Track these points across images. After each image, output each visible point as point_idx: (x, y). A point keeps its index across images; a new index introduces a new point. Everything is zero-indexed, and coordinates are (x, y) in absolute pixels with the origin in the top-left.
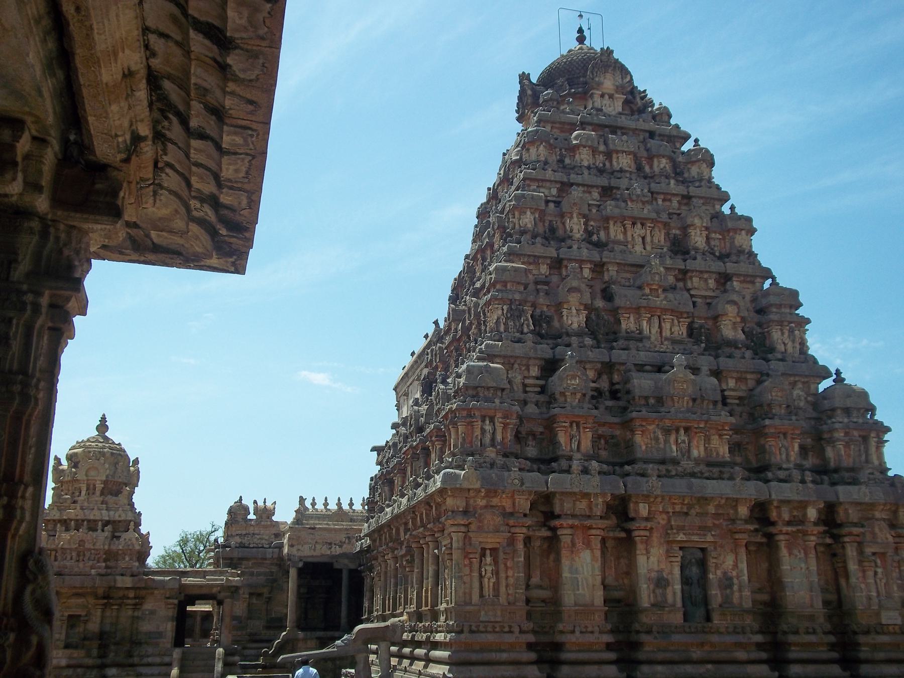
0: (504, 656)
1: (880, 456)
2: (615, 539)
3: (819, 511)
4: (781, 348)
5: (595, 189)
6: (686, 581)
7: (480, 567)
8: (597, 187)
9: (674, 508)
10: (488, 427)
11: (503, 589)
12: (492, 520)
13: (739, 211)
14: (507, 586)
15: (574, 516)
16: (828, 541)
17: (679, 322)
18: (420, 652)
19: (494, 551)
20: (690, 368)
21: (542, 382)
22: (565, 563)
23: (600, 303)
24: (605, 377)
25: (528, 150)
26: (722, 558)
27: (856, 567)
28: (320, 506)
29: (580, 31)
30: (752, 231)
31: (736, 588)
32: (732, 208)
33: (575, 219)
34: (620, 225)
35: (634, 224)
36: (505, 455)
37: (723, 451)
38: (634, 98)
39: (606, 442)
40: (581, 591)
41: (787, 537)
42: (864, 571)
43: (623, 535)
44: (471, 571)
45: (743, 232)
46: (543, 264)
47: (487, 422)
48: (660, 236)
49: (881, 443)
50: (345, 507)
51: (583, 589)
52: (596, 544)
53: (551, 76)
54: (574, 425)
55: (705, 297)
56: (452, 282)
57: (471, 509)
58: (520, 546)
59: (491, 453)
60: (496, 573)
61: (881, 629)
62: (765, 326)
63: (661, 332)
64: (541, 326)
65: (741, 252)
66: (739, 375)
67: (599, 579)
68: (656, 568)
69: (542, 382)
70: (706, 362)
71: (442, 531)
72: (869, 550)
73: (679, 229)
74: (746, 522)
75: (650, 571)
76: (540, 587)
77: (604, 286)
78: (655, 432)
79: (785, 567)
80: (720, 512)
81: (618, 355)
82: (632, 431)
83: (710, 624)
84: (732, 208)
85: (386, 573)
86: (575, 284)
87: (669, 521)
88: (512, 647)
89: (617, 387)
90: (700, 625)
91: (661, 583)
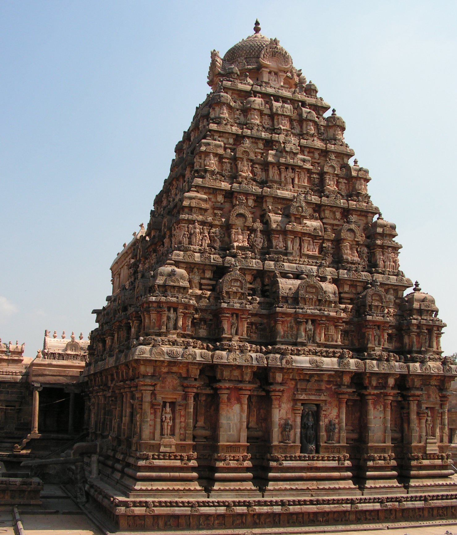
1: (438, 343)
2: (258, 396)
3: (396, 380)
5: (260, 141)
6: (304, 426)
7: (162, 415)
8: (262, 139)
10: (172, 315)
12: (172, 382)
13: (360, 165)
14: (180, 428)
15: (230, 380)
16: (400, 399)
17: (313, 242)
18: (118, 466)
19: (173, 405)
20: (319, 277)
21: (214, 282)
23: (258, 225)
24: (259, 280)
25: (214, 109)
26: (329, 411)
27: (415, 417)
29: (257, 23)
30: (367, 180)
31: (337, 430)
32: (356, 162)
34: (276, 168)
35: (287, 168)
36: (184, 336)
38: (292, 75)
39: (256, 328)
41: (374, 397)
42: (420, 419)
43: (263, 393)
44: (155, 417)
46: (220, 194)
47: (172, 311)
49: (439, 335)
51: (233, 431)
53: (233, 55)
54: (235, 315)
55: (333, 225)
56: (154, 197)
58: (191, 401)
60: (174, 419)
62: (372, 248)
63: (300, 249)
66: (352, 283)
67: (245, 424)
68: (285, 417)
69: (214, 282)
70: (329, 271)
71: (136, 386)
73: (318, 174)
74: (348, 387)
76: (203, 428)
77: (263, 213)
78: (291, 323)
81: (270, 265)
82: (276, 322)
84: (356, 162)
85: (98, 404)
86: (242, 211)
87: (296, 385)
89: (267, 288)
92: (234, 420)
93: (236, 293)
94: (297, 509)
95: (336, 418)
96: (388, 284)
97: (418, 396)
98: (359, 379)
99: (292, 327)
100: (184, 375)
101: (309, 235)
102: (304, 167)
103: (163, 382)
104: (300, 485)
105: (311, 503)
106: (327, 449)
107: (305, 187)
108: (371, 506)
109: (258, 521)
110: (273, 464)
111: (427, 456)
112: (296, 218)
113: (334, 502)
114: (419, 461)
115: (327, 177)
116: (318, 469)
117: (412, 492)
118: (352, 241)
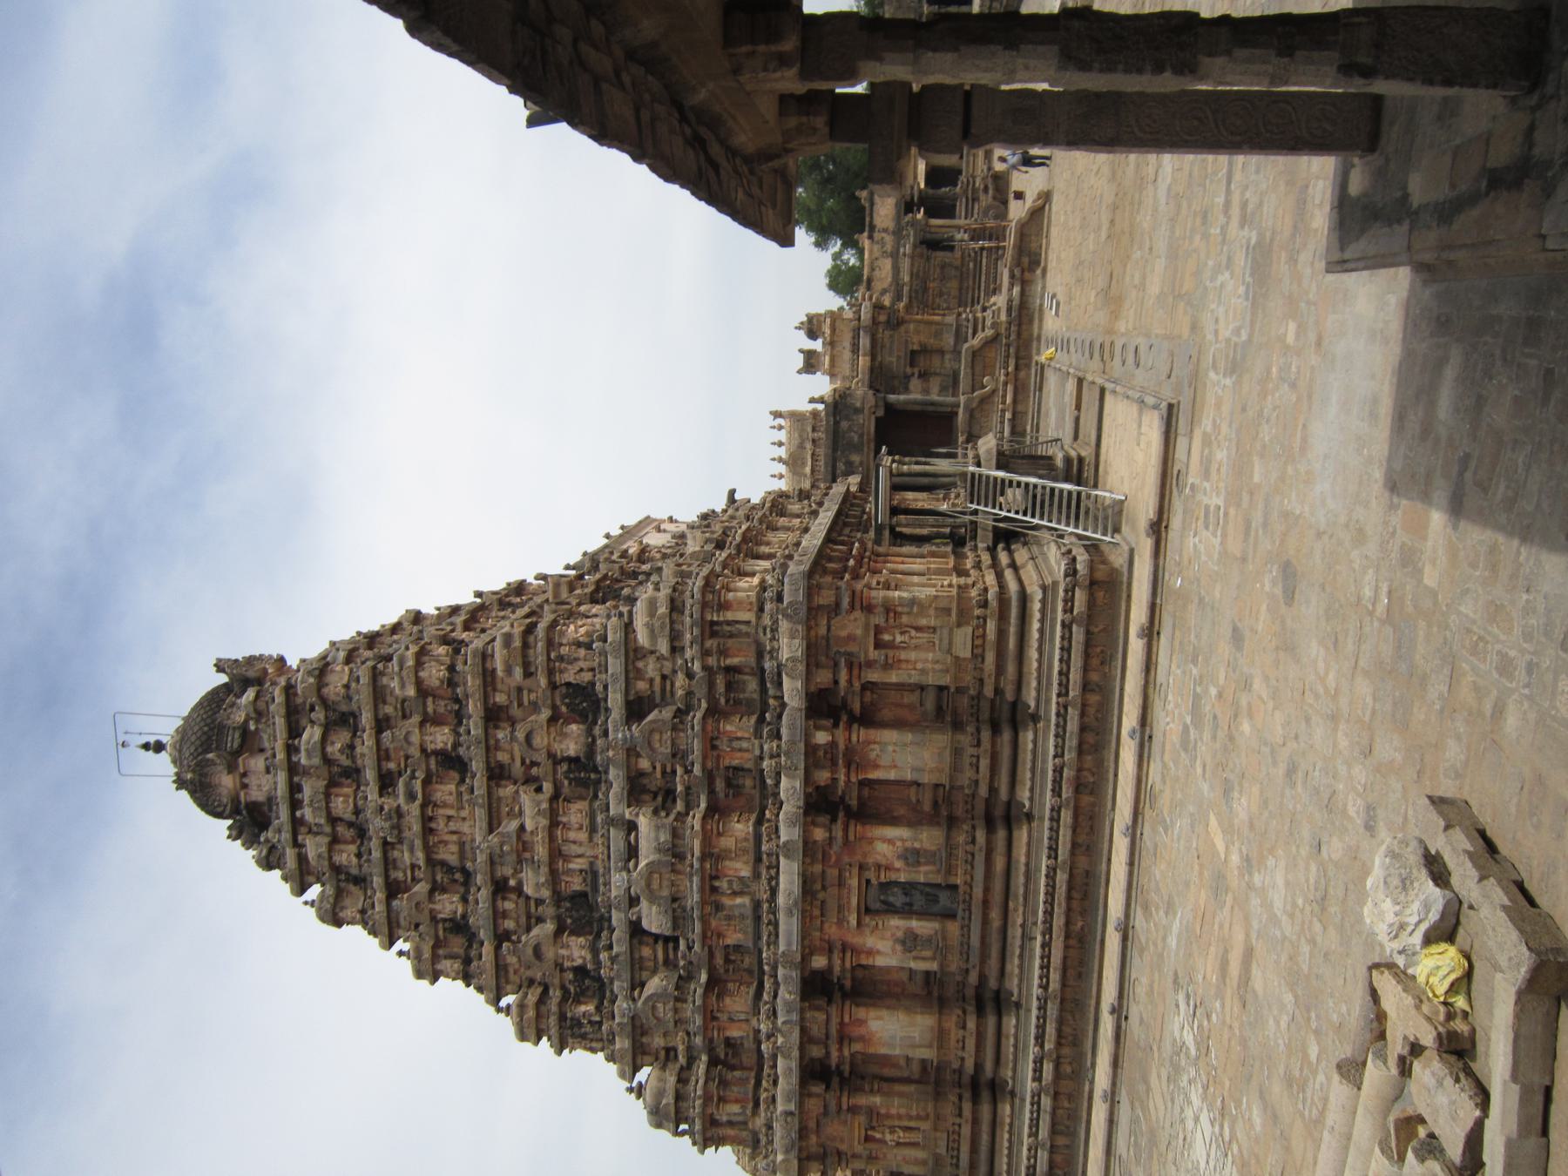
0: (985, 1138)
3: (817, 728)
4: (587, 677)
6: (907, 911)
11: (912, 1124)
12: (833, 1128)
14: (910, 1118)
22: (883, 1051)
28: (782, 436)
29: (146, 746)
31: (917, 845)
33: (437, 907)
35: (431, 830)
37: (740, 828)
45: (421, 674)
48: (445, 791)
50: (782, 452)
52: (861, 1013)
58: (862, 1100)
61: (978, 657)
65: (451, 683)
68: (890, 943)
75: (893, 950)
79: (892, 775)
83: (961, 890)
88: (976, 1121)
91: (910, 942)
92: (894, 1031)
93: (676, 1011)
94: (1055, 976)
96: (627, 671)
97: (850, 666)
98: (819, 804)
99: (729, 918)
101: (554, 824)
102: (420, 796)
104: (1015, 933)
106: (950, 871)
107: (460, 794)
110: (973, 978)
111: (978, 657)
112: (525, 850)
113: (1050, 902)
114: (987, 681)
115: (430, 747)
116: (987, 890)
117: (1047, 711)
118: (549, 733)
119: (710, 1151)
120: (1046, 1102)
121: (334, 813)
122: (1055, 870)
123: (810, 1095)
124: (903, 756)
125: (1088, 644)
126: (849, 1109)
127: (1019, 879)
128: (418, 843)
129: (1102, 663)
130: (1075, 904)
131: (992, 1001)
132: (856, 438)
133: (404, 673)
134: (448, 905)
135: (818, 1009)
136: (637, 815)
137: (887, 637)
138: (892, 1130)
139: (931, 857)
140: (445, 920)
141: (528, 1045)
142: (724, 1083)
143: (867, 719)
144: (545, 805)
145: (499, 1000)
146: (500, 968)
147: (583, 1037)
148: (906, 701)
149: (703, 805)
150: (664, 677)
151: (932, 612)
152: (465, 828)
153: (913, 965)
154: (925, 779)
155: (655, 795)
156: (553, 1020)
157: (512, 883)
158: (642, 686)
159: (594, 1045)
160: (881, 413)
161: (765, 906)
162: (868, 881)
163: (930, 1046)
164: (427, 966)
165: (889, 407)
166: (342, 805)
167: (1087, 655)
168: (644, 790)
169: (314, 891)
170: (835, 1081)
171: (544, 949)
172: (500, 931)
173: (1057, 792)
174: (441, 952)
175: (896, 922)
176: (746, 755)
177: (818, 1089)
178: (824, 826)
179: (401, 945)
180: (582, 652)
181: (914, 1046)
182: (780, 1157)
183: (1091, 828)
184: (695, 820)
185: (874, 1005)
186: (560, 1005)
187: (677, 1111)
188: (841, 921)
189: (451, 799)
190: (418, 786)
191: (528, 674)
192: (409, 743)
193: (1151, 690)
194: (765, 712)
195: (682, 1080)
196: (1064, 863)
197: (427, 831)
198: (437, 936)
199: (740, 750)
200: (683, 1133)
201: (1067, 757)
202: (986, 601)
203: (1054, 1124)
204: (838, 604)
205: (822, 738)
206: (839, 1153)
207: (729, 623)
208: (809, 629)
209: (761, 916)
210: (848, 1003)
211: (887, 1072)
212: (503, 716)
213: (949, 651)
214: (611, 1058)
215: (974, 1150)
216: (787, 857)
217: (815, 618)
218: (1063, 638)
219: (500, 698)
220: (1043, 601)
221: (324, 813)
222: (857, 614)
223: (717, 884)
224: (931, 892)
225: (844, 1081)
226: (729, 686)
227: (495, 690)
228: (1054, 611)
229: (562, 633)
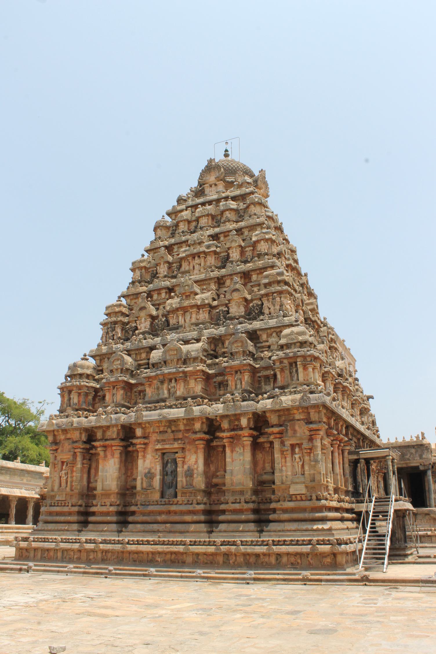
0: (62, 518)
3: (249, 419)
6: (164, 473)
9: (159, 429)
11: (69, 483)
12: (67, 446)
14: (72, 482)
22: (100, 467)
29: (226, 151)
31: (195, 476)
33: (162, 266)
40: (108, 483)
42: (286, 458)
45: (262, 242)
48: (211, 260)
51: (109, 481)
52: (117, 454)
57: (58, 441)
58: (79, 459)
59: (70, 411)
64: (129, 333)
65: (259, 256)
68: (149, 466)
72: (288, 443)
79: (228, 460)
80: (187, 428)
88: (70, 514)
90: (167, 500)
91: (149, 475)
92: (109, 471)
93: (117, 370)
94: (133, 548)
95: (195, 464)
100: (75, 440)
101: (199, 307)
103: (63, 447)
104: (155, 527)
105: (148, 543)
106: (184, 493)
108: (204, 549)
109: (105, 558)
114: (279, 504)
115: (230, 251)
116: (175, 513)
118: (239, 299)
119: (59, 391)
120: (76, 546)
121: (201, 220)
122: (184, 545)
123: (81, 433)
124: (238, 465)
125: (300, 555)
126: (75, 453)
127: (179, 527)
128: (188, 253)
129: (292, 564)
130: (168, 556)
131: (124, 519)
132: (407, 457)
133: (262, 235)
134: (163, 270)
135: (118, 434)
136: (203, 341)
137: (297, 450)
138: (66, 474)
139: (190, 484)
140: (156, 270)
141: (104, 310)
142: (87, 395)
143: (256, 446)
144: (207, 302)
145: (124, 297)
146: (137, 295)
147: (107, 333)
148: (267, 465)
149: (210, 372)
150: (269, 347)
151: (312, 472)
152: (196, 271)
153: (139, 478)
154: (228, 477)
155: (215, 351)
156: (114, 319)
157: (173, 294)
158: (264, 337)
159: (104, 338)
160: (421, 468)
161: (163, 404)
162: (177, 453)
163: (102, 490)
164: (137, 265)
165: (425, 472)
166: (203, 222)
167: (296, 554)
168: (216, 346)
169: (168, 219)
170: (88, 446)
171: (144, 311)
172: (152, 293)
173: (223, 544)
174: (143, 270)
175: (158, 468)
176: (234, 387)
177: (84, 438)
178: (202, 428)
179: (146, 254)
180: (278, 307)
181: (103, 482)
182: (54, 422)
183: (206, 563)
184: (201, 367)
185: (121, 462)
186: (121, 321)
187: (75, 375)
188: (158, 441)
189: (208, 264)
190: (213, 249)
191: (266, 285)
192: (232, 241)
193: (273, 582)
194: (255, 391)
195: (88, 376)
196: (188, 549)
197: (193, 256)
198: (150, 268)
199: (236, 385)
200: (66, 379)
201: (241, 547)
202: (320, 500)
203: (67, 550)
204: (311, 423)
205: (244, 422)
206: (56, 450)
207: (297, 371)
208: (297, 408)
209: (159, 402)
210: (121, 448)
211: (93, 471)
212: (247, 280)
213: (293, 483)
214: (99, 345)
215: (58, 514)
216: (185, 411)
217: (303, 412)
218: (303, 541)
219: (254, 277)
220: (323, 530)
221: (200, 215)
222: (308, 433)
223: (173, 381)
224: (173, 484)
225: (88, 450)
226: (267, 378)
227: (258, 274)
228: (318, 535)
229: (286, 298)
